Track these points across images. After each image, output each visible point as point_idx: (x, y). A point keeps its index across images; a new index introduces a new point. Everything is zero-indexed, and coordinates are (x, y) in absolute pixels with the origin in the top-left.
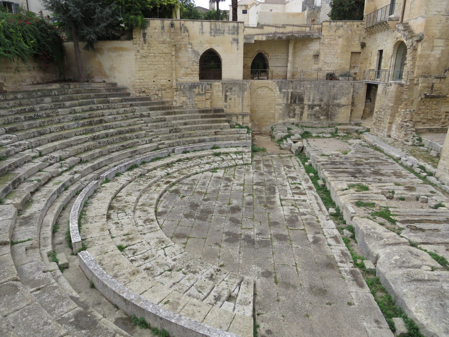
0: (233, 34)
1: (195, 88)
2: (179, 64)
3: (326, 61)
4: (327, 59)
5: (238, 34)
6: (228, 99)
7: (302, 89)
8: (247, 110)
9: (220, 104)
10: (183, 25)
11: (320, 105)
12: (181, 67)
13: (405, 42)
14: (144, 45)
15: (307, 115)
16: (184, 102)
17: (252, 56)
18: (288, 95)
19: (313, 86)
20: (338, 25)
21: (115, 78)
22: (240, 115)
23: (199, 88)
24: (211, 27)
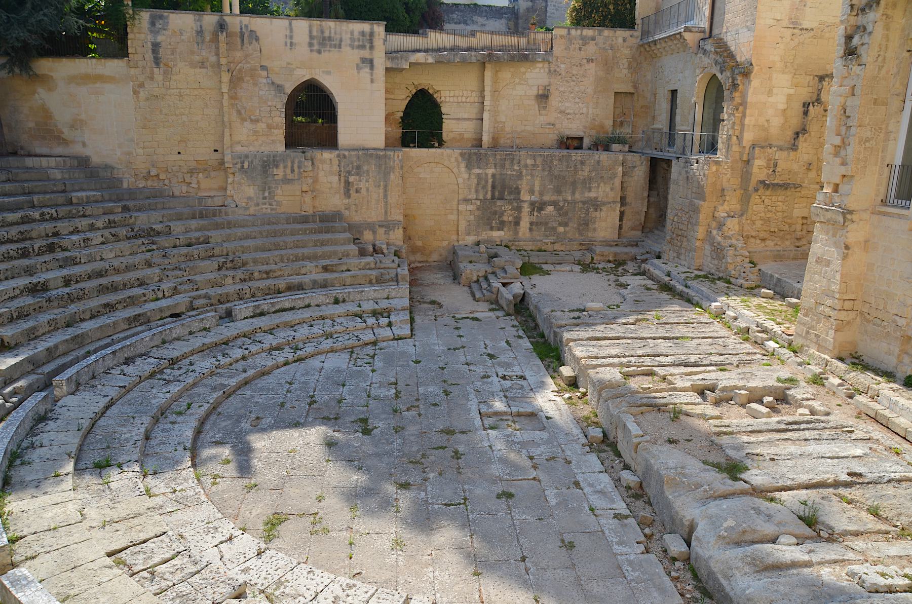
0: (363, 47)
1: (277, 167)
2: (239, 113)
3: (563, 108)
4: (567, 104)
6: (352, 192)
7: (516, 167)
8: (397, 216)
9: (333, 201)
10: (246, 26)
11: (554, 204)
12: (244, 120)
13: (719, 76)
14: (156, 70)
15: (528, 225)
16: (250, 198)
17: (404, 97)
18: (487, 182)
19: (539, 161)
20: (586, 37)
21: (84, 145)
23: (285, 167)
24: (310, 32)
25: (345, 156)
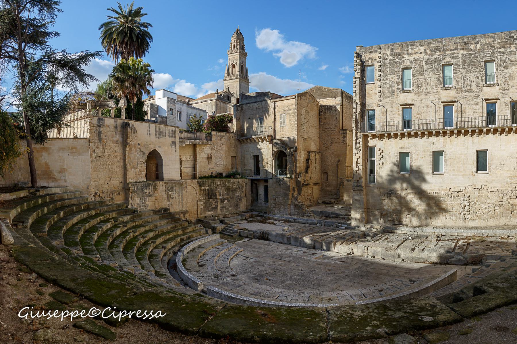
0: (172, 137)
5: (175, 137)
6: (170, 199)
9: (165, 204)
13: (285, 151)
16: (138, 204)
22: (182, 213)
23: (149, 189)
25: (167, 183)
